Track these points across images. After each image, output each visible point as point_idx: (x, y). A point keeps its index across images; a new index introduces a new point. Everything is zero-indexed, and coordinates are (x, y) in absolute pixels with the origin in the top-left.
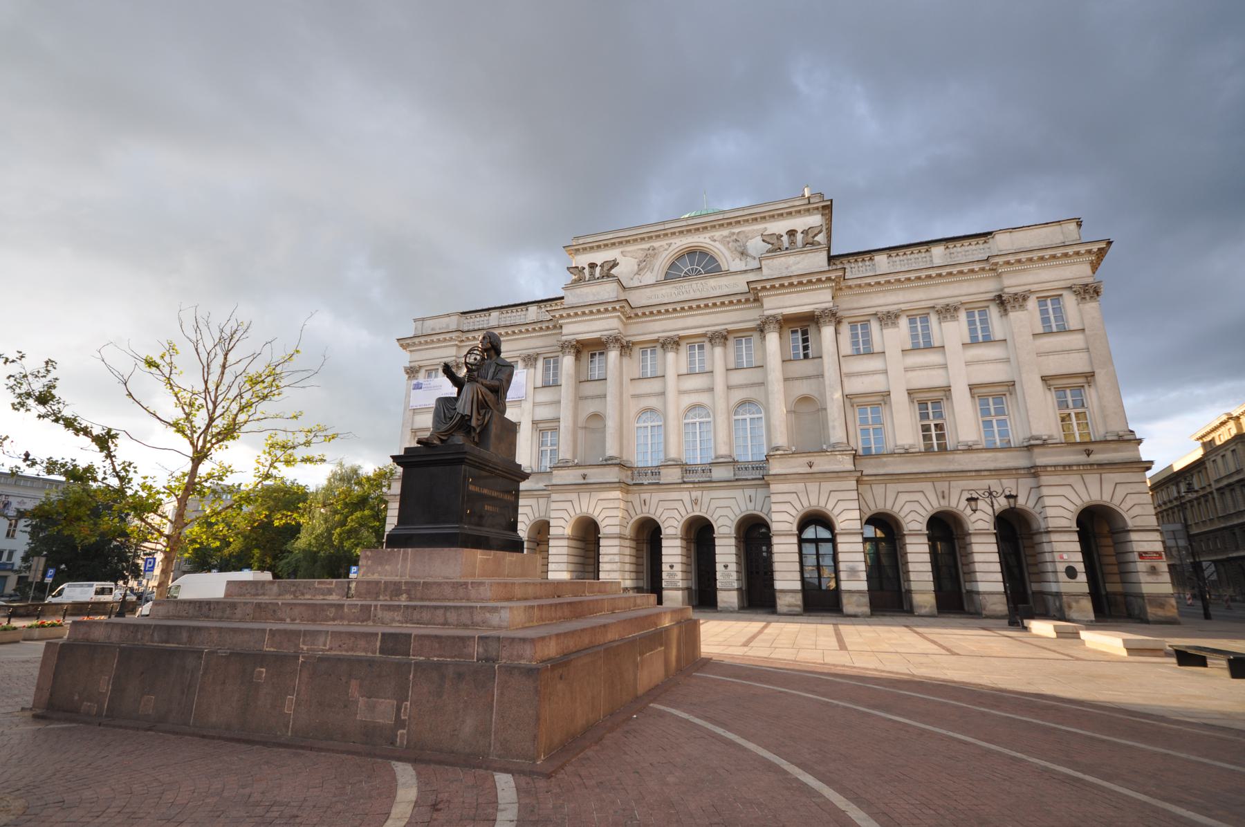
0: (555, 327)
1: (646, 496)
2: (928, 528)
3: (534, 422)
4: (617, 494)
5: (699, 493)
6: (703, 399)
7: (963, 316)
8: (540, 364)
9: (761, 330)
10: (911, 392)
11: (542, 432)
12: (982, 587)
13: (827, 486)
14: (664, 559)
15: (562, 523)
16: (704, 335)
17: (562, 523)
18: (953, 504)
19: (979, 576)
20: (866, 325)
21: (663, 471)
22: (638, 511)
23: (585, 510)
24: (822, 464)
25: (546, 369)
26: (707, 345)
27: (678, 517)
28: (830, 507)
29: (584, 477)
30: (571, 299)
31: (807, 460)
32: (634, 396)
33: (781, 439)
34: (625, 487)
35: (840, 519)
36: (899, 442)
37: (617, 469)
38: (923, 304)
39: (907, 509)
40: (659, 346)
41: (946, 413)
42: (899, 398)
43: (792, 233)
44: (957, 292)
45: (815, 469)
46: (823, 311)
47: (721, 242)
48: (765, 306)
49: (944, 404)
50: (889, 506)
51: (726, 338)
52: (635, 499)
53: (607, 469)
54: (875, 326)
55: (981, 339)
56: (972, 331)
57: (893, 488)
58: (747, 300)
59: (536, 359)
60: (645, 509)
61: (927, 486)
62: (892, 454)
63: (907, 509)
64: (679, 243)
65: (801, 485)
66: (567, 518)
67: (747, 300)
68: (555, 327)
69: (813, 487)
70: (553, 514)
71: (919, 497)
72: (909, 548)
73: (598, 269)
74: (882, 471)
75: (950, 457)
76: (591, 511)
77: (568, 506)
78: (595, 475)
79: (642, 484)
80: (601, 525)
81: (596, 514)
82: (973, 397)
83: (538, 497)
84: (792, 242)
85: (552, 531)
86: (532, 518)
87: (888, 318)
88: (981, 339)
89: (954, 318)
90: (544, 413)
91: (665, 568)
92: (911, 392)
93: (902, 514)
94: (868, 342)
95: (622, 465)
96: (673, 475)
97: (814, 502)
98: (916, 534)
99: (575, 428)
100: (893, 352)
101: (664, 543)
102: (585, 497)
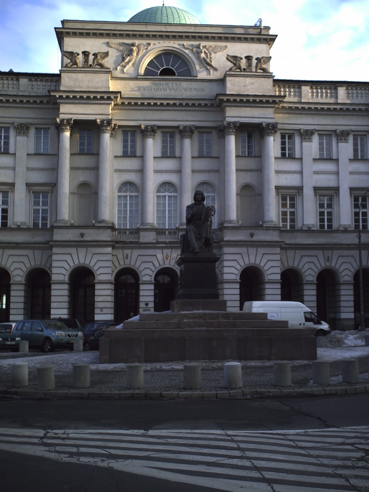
0: (48, 102)
1: (128, 252)
2: (317, 280)
3: (28, 185)
4: (109, 250)
5: (169, 251)
6: (173, 178)
7: (351, 139)
8: (32, 132)
9: (222, 131)
10: (316, 189)
11: (36, 194)
12: (343, 316)
13: (262, 250)
14: (141, 299)
15: (63, 271)
16: (178, 127)
17: (63, 271)
18: (333, 265)
19: (342, 309)
20: (291, 137)
21: (142, 234)
22: (122, 263)
23: (82, 261)
24: (260, 236)
25: (38, 138)
26: (177, 137)
27: (153, 268)
28: (262, 264)
29: (82, 235)
30: (68, 82)
31: (249, 231)
32: (116, 171)
33: (233, 214)
34: (115, 244)
35: (269, 272)
36: (305, 223)
37: (109, 231)
38: (329, 128)
39: (306, 267)
40: (138, 131)
41: (335, 206)
42: (308, 192)
43: (249, 58)
44: (350, 123)
45: (255, 238)
46: (268, 124)
47: (192, 50)
48: (228, 114)
49: (335, 199)
50: (296, 265)
51: (192, 132)
52: (119, 253)
53: (100, 231)
54: (297, 140)
55: (360, 157)
56: (355, 150)
57: (299, 253)
58: (212, 105)
59: (28, 128)
60: (127, 262)
61: (319, 253)
62: (301, 231)
63: (306, 267)
64: (158, 45)
65: (244, 250)
66: (67, 267)
67: (212, 105)
68: (48, 102)
69: (252, 251)
70: (54, 264)
71: (314, 259)
72: (306, 292)
73: (91, 57)
74: (293, 242)
75: (335, 235)
76: (87, 262)
77: (68, 258)
78: (91, 235)
79: (124, 242)
80: (97, 273)
81: (92, 265)
82: (351, 196)
83: (33, 249)
84: (250, 65)
85: (54, 278)
86: (28, 266)
87: (307, 135)
88: (360, 157)
89: (346, 141)
90: (37, 177)
91: (142, 305)
92: (316, 189)
93: (303, 270)
94: (292, 149)
95: (112, 228)
96: (148, 237)
97: (252, 261)
98: (310, 283)
99: (71, 193)
100: (308, 160)
101: (142, 287)
102: (82, 251)
